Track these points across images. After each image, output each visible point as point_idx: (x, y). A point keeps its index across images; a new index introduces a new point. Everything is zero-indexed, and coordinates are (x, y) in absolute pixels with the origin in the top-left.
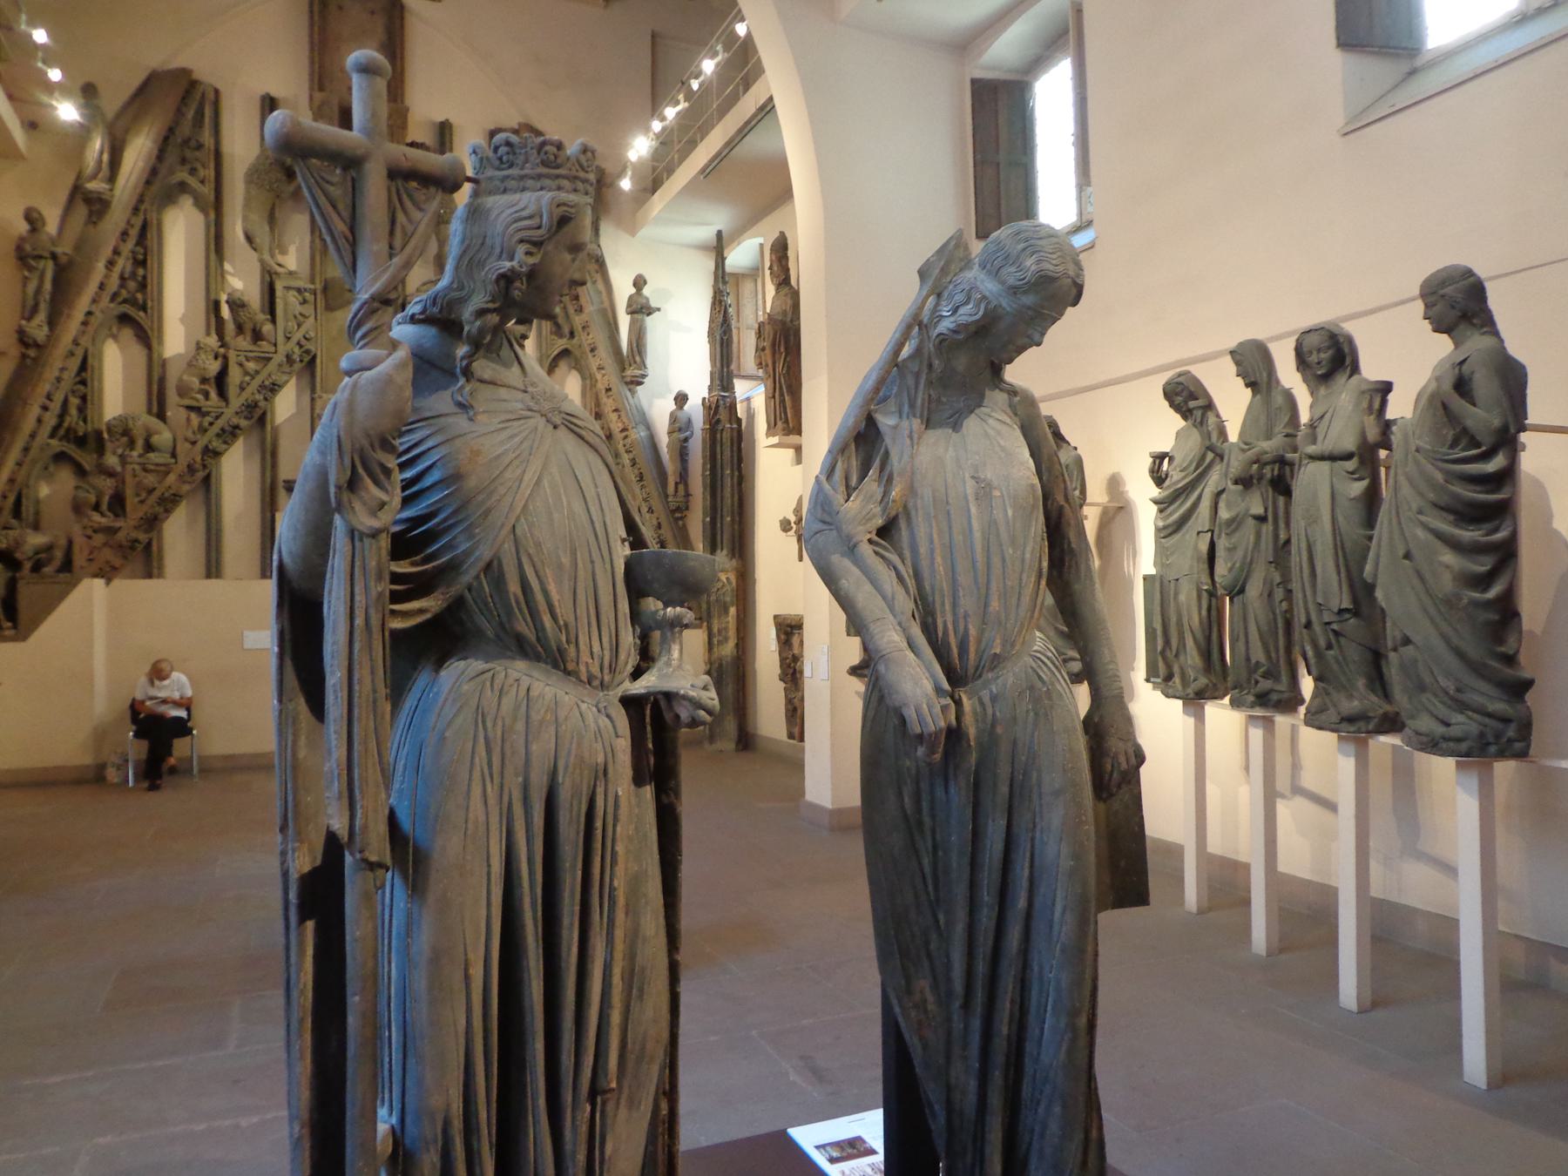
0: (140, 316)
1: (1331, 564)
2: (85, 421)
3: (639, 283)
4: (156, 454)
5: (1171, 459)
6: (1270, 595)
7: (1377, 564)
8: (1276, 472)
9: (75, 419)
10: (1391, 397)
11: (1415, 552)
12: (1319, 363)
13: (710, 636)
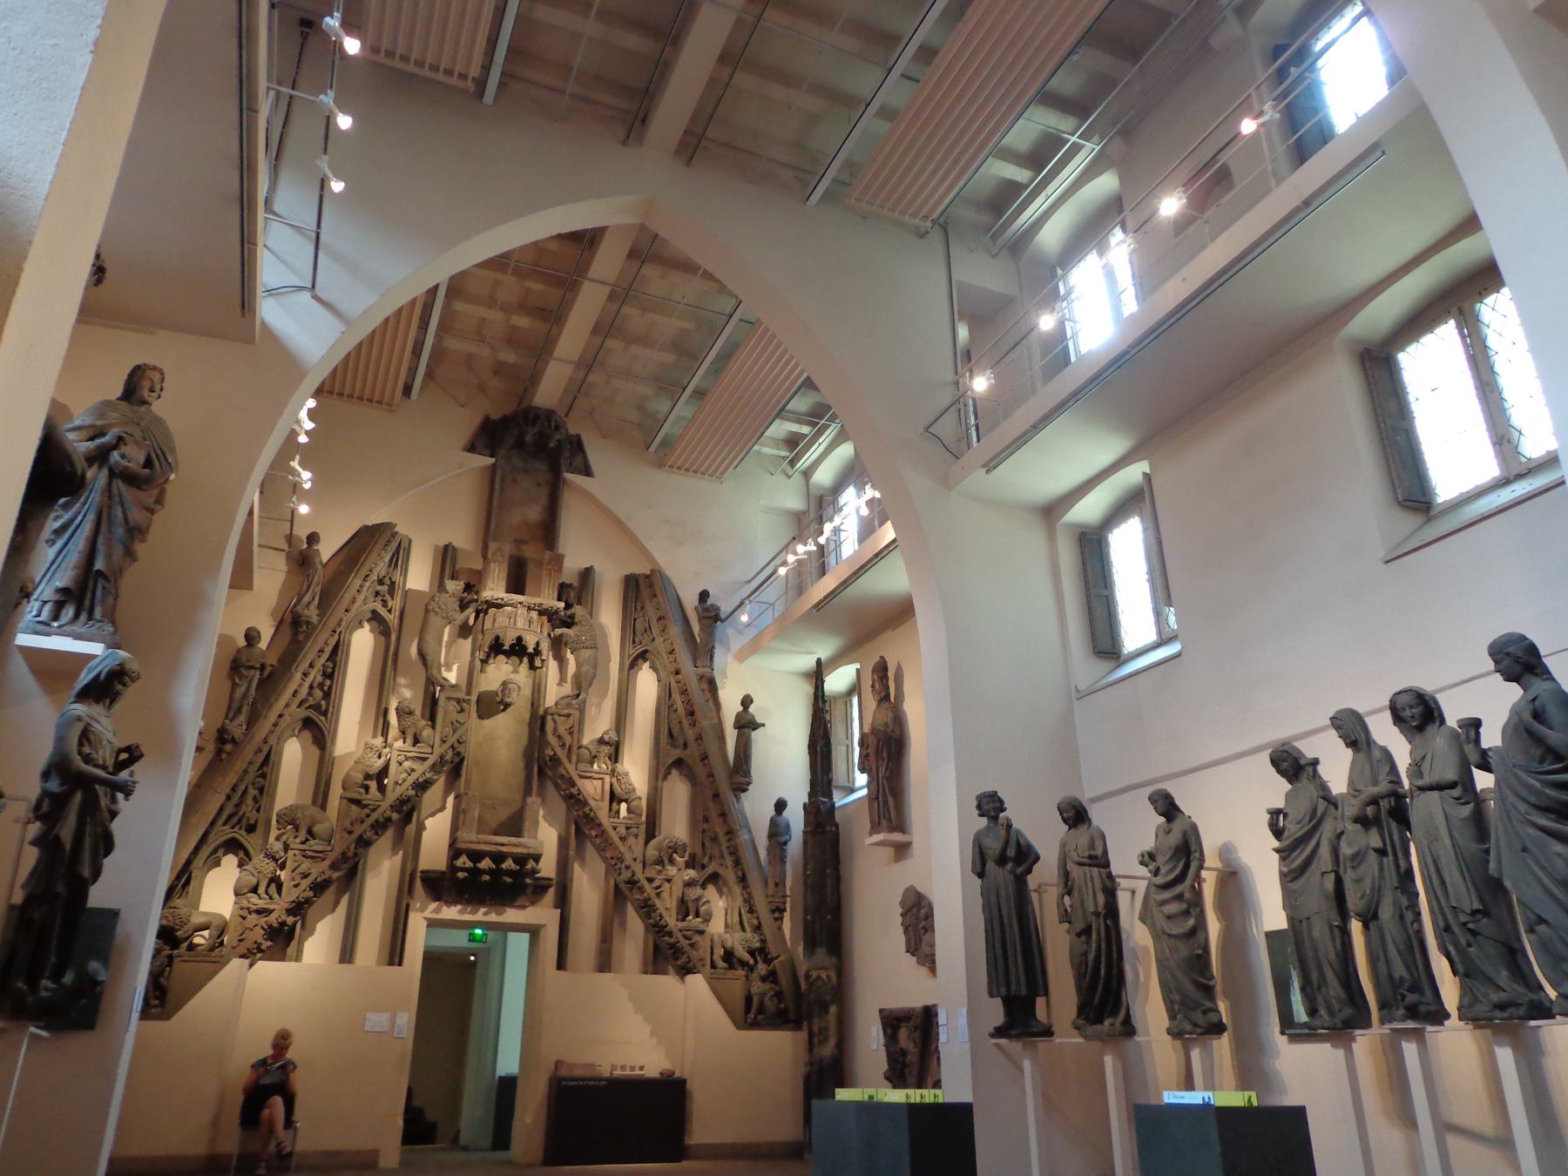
0: (320, 719)
1: (1457, 874)
2: (258, 811)
3: (747, 702)
4: (316, 841)
5: (1285, 816)
6: (1402, 917)
7: (1499, 862)
8: (1393, 804)
9: (250, 807)
10: (1481, 730)
11: (1529, 845)
12: (1412, 717)
13: (811, 1035)
